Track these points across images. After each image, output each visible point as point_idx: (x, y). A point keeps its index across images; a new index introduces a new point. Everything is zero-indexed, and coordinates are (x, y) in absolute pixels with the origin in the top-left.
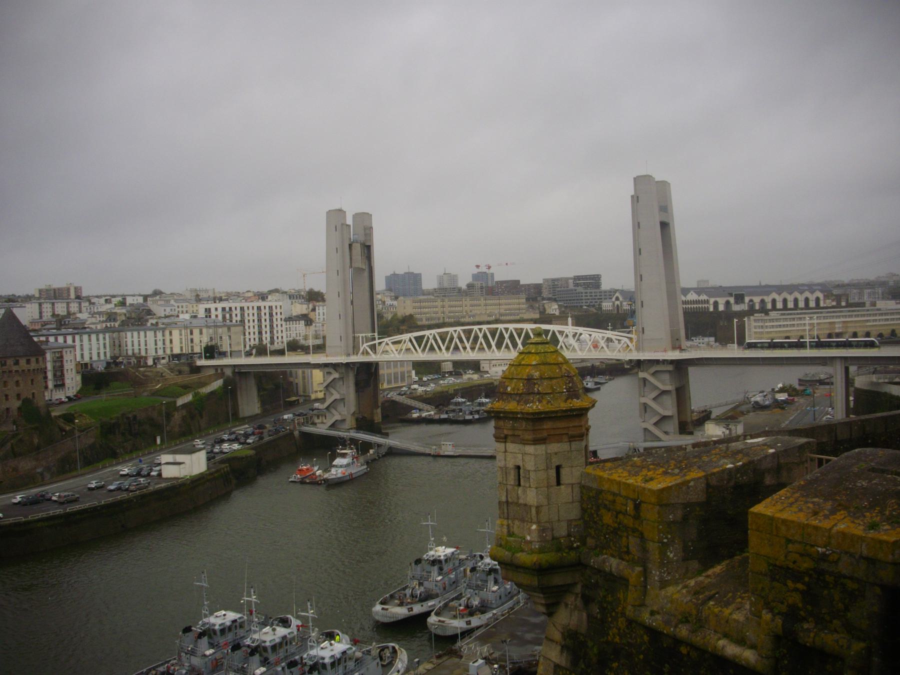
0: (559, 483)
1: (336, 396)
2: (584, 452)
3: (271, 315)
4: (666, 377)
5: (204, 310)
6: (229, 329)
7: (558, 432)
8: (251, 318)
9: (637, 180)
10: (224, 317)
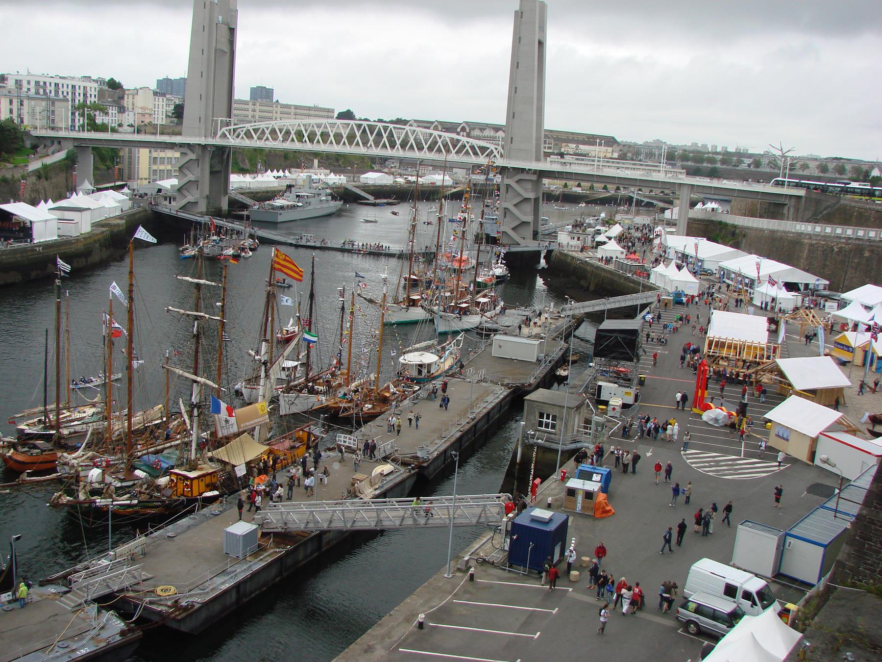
1: (191, 177)
4: (529, 186)
6: (53, 104)
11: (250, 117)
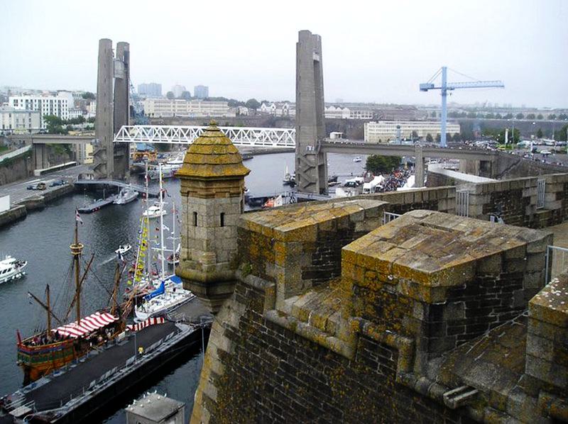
0: (222, 225)
2: (240, 204)
3: (59, 106)
6: (30, 114)
7: (223, 190)
8: (46, 107)
9: (301, 33)
10: (27, 106)
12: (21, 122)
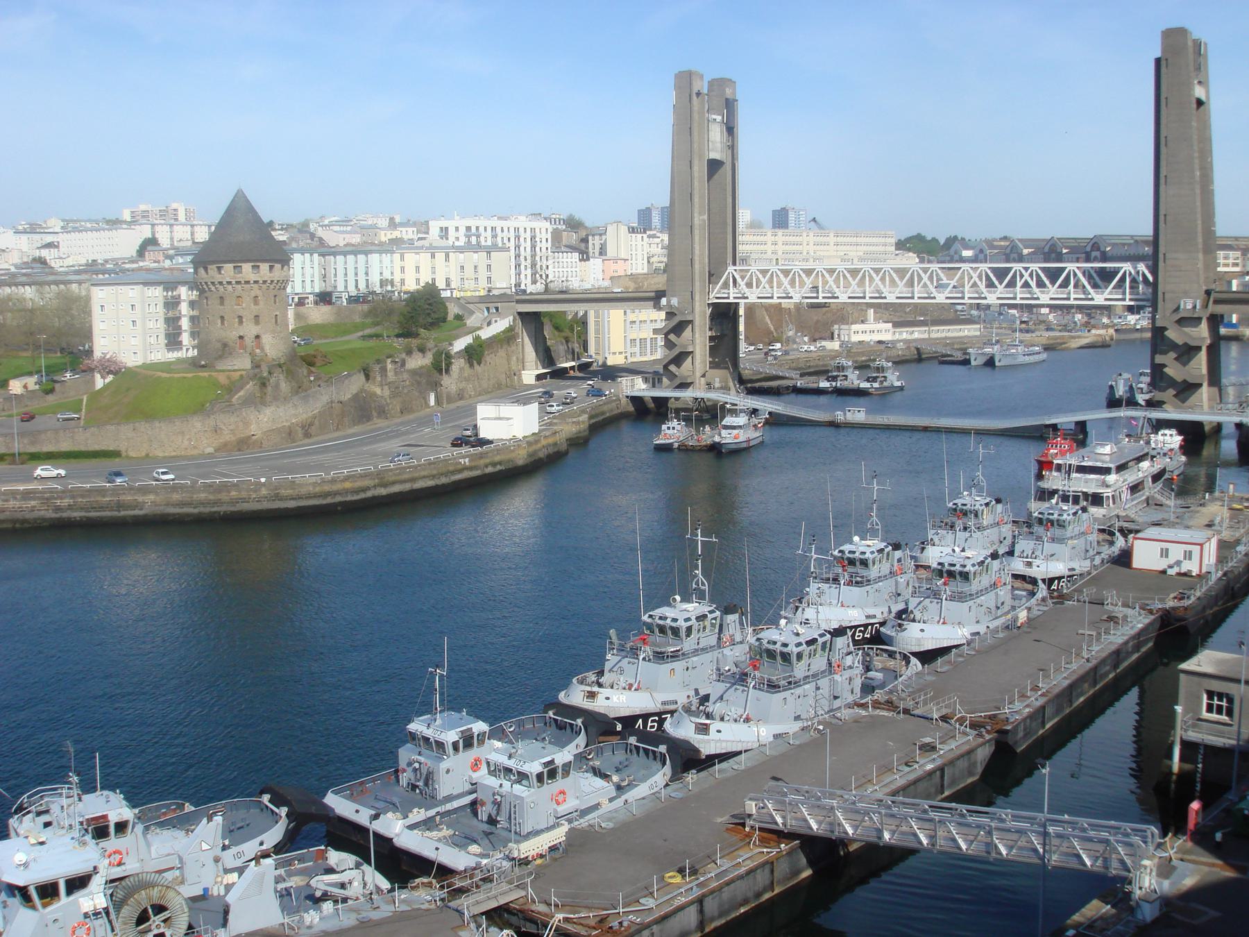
5: (439, 229)
11: (769, 252)
12: (469, 272)
